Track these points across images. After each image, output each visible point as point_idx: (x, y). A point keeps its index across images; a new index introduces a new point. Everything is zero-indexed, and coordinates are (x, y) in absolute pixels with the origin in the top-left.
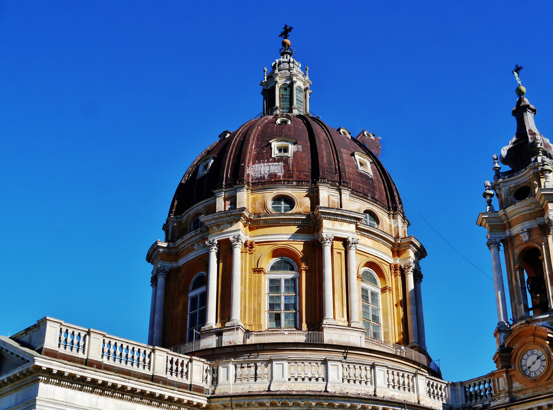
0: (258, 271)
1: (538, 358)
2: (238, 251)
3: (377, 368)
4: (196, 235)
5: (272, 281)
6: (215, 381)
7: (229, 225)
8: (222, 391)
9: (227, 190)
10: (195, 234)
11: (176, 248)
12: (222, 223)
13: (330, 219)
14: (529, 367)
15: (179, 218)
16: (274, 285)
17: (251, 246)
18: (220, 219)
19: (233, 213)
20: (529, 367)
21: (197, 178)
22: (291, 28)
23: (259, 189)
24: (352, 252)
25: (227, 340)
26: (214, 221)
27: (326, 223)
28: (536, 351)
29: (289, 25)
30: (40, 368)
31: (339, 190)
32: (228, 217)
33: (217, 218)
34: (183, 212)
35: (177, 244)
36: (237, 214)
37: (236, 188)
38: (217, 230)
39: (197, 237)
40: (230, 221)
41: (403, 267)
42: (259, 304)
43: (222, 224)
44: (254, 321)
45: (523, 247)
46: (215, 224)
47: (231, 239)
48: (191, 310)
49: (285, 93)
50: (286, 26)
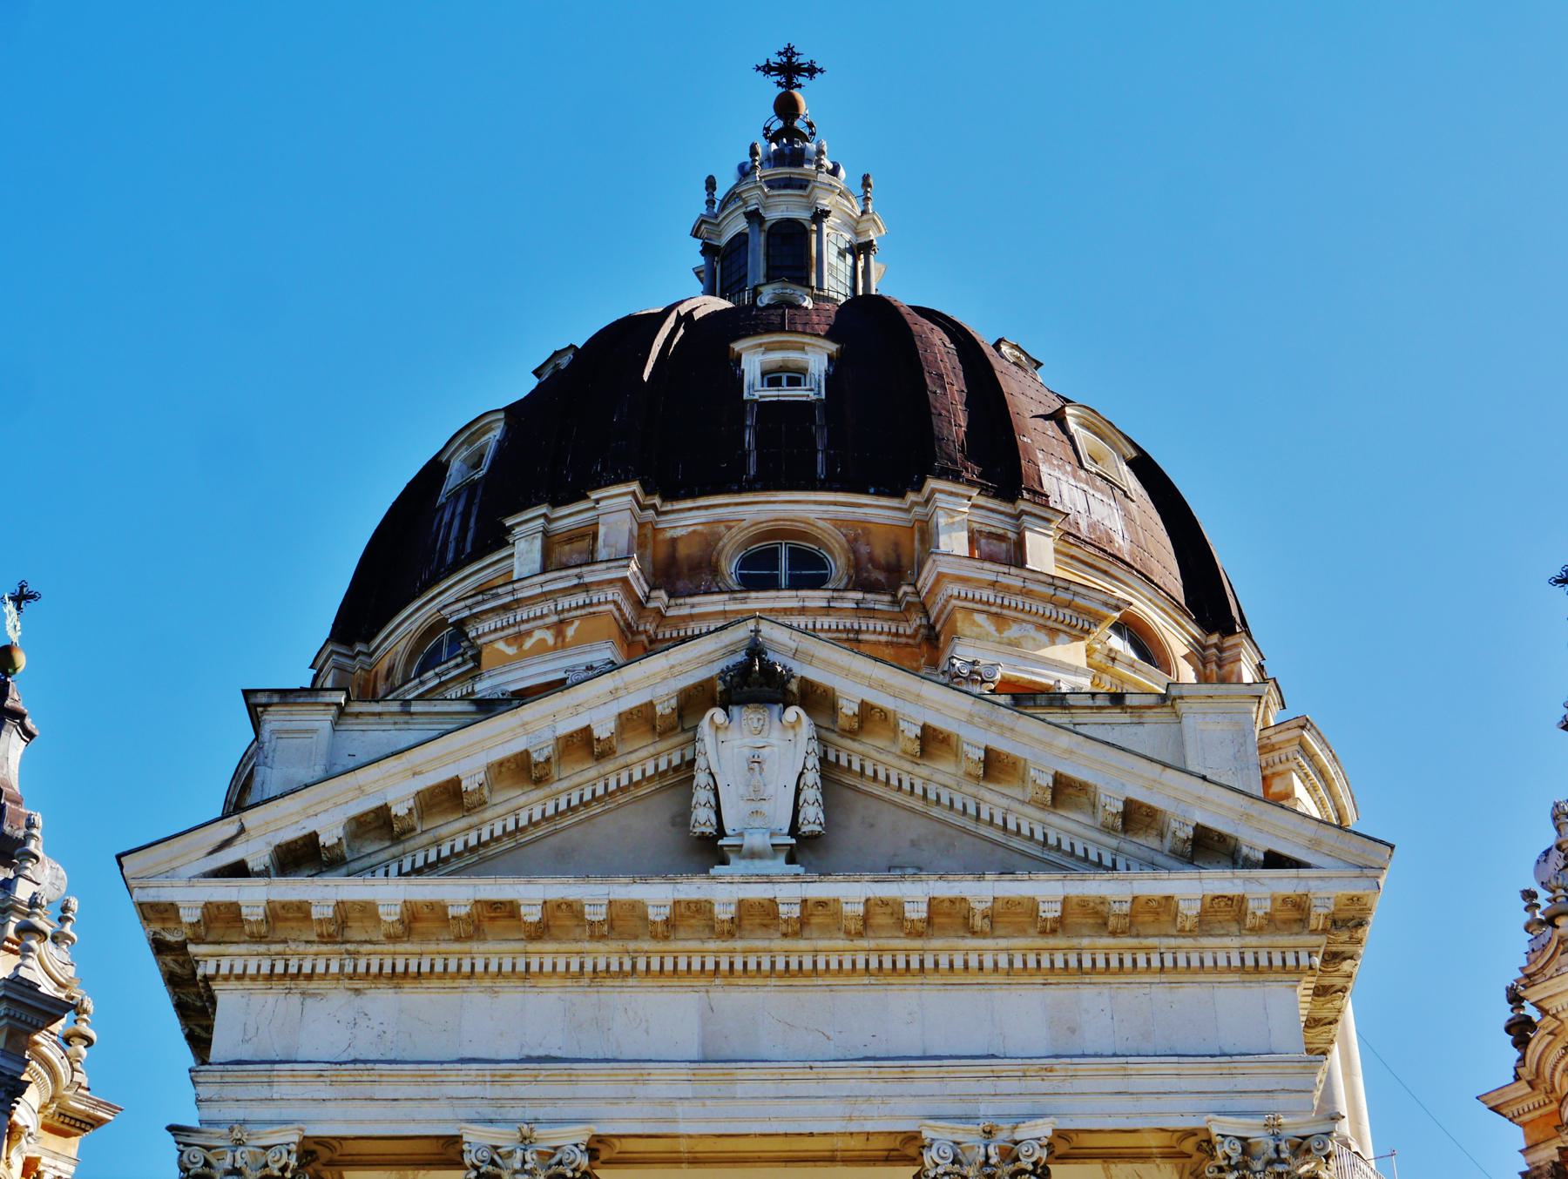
4: (828, 610)
7: (1042, 636)
9: (982, 501)
10: (825, 604)
12: (1021, 616)
15: (654, 506)
18: (1019, 598)
19: (1078, 600)
23: (1072, 557)
26: (987, 594)
32: (1050, 606)
33: (1007, 589)
34: (692, 495)
35: (685, 611)
36: (1088, 612)
37: (1023, 512)
38: (996, 634)
39: (825, 622)
40: (1051, 624)
43: (1015, 620)
46: (986, 608)
49: (841, 266)
50: (789, 52)
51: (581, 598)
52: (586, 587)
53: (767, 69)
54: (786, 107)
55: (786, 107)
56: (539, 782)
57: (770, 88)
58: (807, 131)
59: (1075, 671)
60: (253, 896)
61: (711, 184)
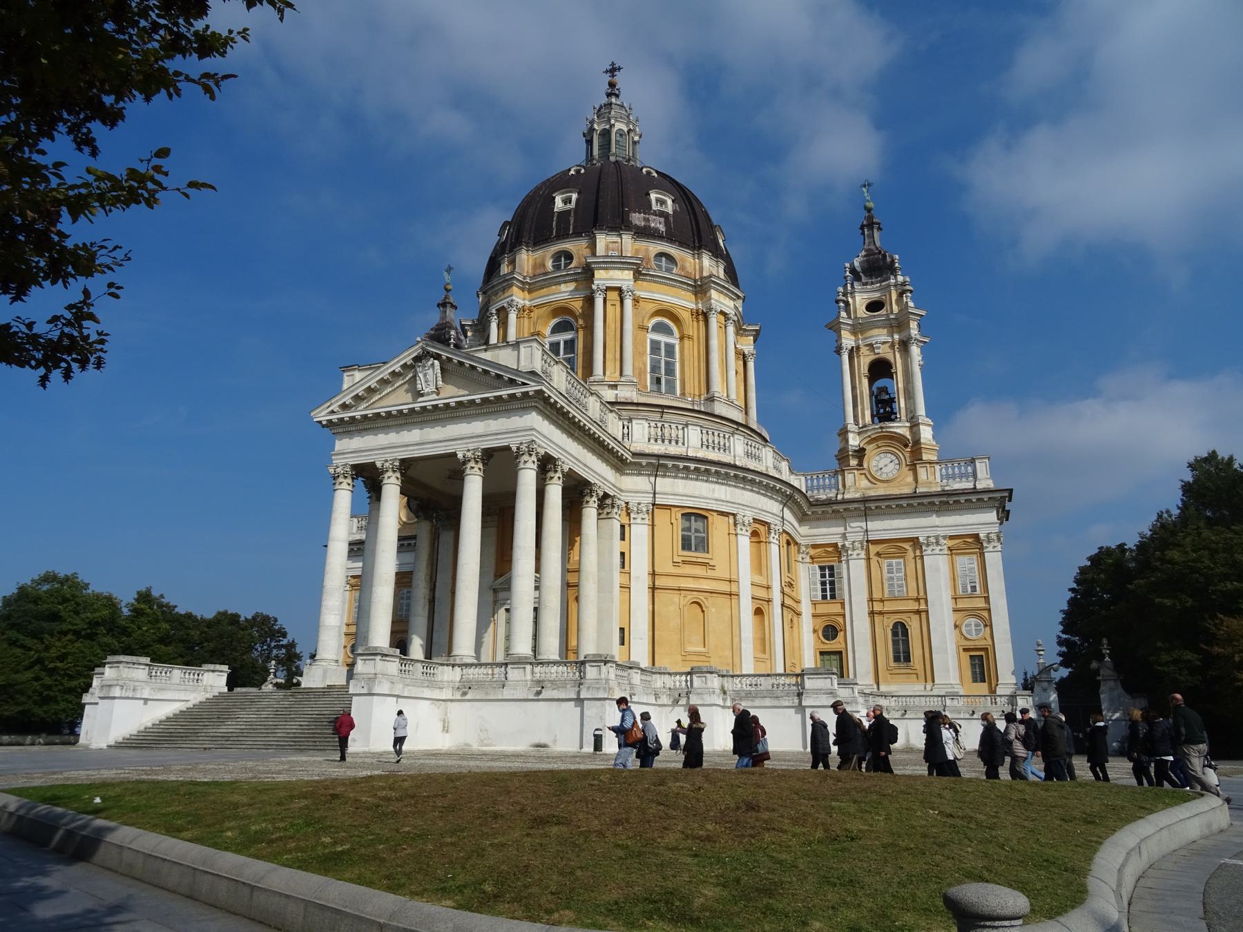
0: (643, 328)
1: (891, 462)
2: (628, 303)
5: (652, 341)
6: (627, 435)
8: (638, 448)
11: (529, 284)
14: (881, 469)
16: (655, 346)
20: (881, 469)
21: (555, 210)
22: (619, 69)
25: (622, 395)
27: (714, 294)
28: (890, 455)
41: (746, 352)
42: (645, 365)
44: (640, 379)
45: (873, 357)
47: (624, 288)
50: (613, 64)
51: (506, 284)
52: (507, 280)
53: (607, 72)
54: (612, 85)
55: (612, 85)
56: (390, 382)
57: (607, 78)
58: (617, 92)
59: (629, 280)
60: (334, 417)
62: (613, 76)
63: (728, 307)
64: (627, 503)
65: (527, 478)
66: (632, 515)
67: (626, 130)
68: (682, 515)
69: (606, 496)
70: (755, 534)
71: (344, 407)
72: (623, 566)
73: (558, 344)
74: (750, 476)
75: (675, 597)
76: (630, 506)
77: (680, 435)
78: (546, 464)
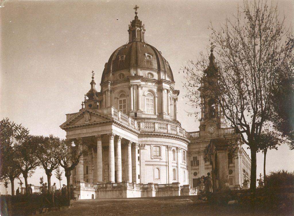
0: (144, 95)
3: (168, 125)
13: (165, 83)
17: (142, 88)
24: (169, 94)
27: (164, 84)
29: (138, 6)
30: (114, 121)
31: (165, 74)
47: (138, 85)
48: (120, 104)
50: (136, 6)
53: (134, 9)
55: (136, 13)
61: (129, 25)
62: (136, 10)
63: (168, 87)
64: (139, 144)
65: (112, 142)
66: (141, 147)
67: (140, 29)
68: (154, 146)
69: (133, 143)
70: (173, 150)
71: (67, 125)
72: (139, 160)
73: (122, 100)
74: (172, 135)
75: (152, 167)
76: (140, 145)
77: (153, 126)
78: (117, 138)
